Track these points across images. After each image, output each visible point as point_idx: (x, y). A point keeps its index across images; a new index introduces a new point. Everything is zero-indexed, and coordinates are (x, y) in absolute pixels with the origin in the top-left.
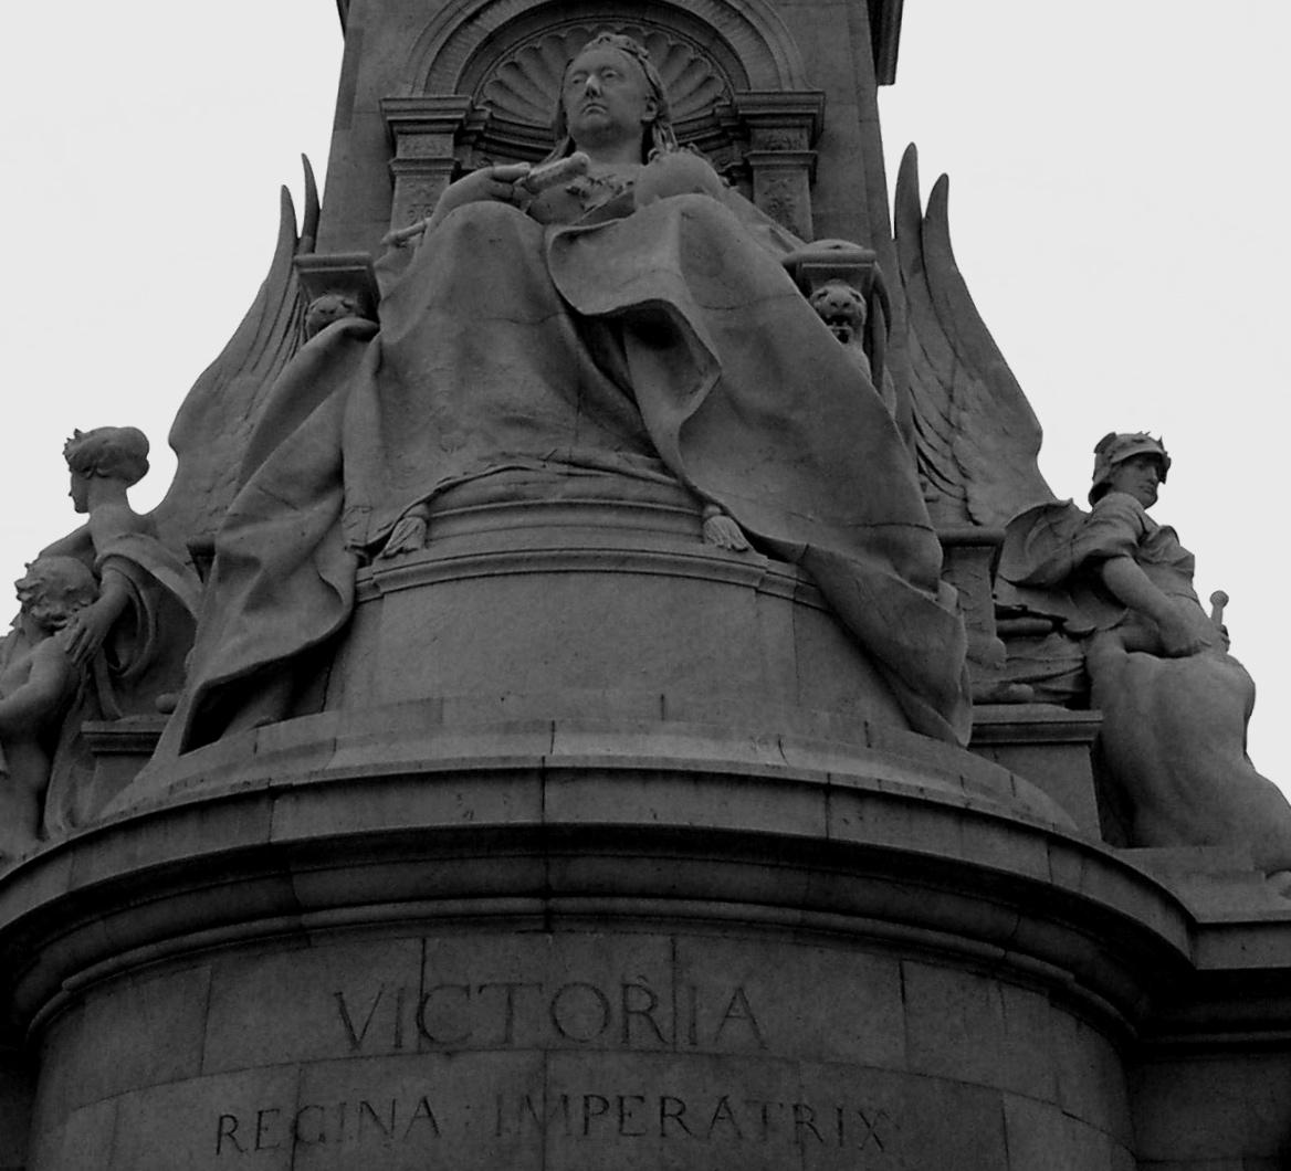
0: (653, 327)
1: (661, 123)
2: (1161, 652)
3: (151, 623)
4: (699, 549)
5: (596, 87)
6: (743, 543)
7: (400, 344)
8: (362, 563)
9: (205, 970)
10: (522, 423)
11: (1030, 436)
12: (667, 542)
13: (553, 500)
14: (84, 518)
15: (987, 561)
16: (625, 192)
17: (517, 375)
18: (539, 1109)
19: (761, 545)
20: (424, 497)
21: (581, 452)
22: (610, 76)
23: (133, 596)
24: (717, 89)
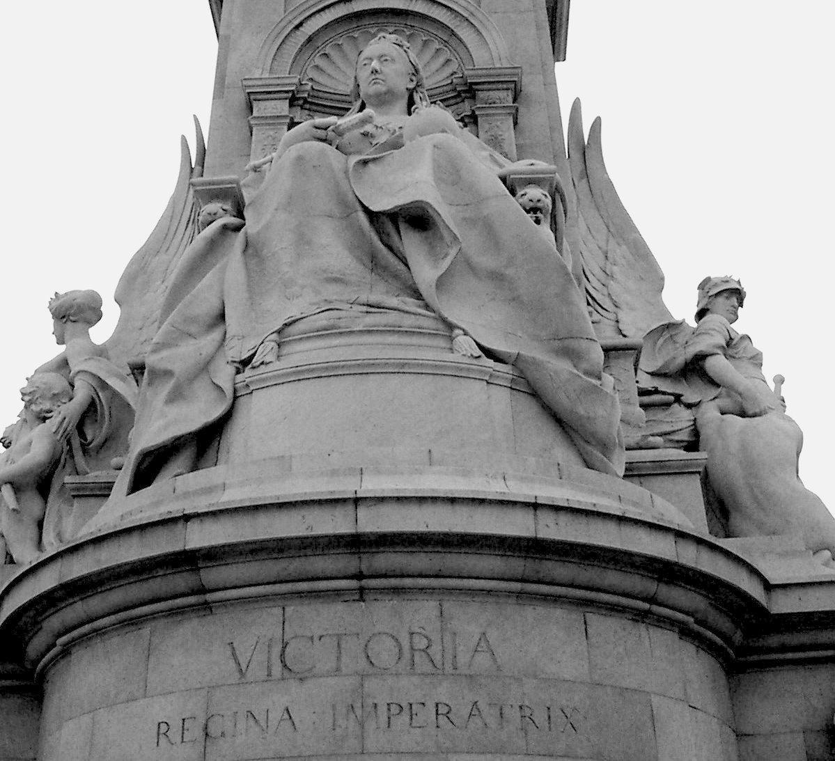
0: (418, 219)
1: (419, 89)
2: (743, 414)
3: (107, 413)
4: (449, 357)
5: (378, 68)
6: (478, 352)
7: (258, 233)
8: (238, 372)
9: (146, 631)
10: (336, 280)
11: (657, 282)
12: (430, 352)
13: (358, 329)
14: (62, 349)
15: (632, 360)
16: (397, 133)
17: (334, 250)
18: (359, 712)
19: (489, 353)
20: (276, 329)
21: (374, 298)
22: (386, 60)
23: (95, 396)
24: (454, 67)
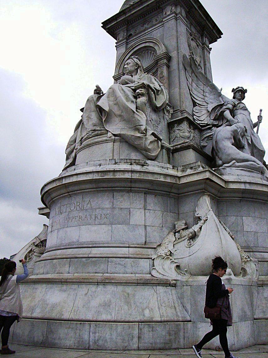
6: (112, 135)
